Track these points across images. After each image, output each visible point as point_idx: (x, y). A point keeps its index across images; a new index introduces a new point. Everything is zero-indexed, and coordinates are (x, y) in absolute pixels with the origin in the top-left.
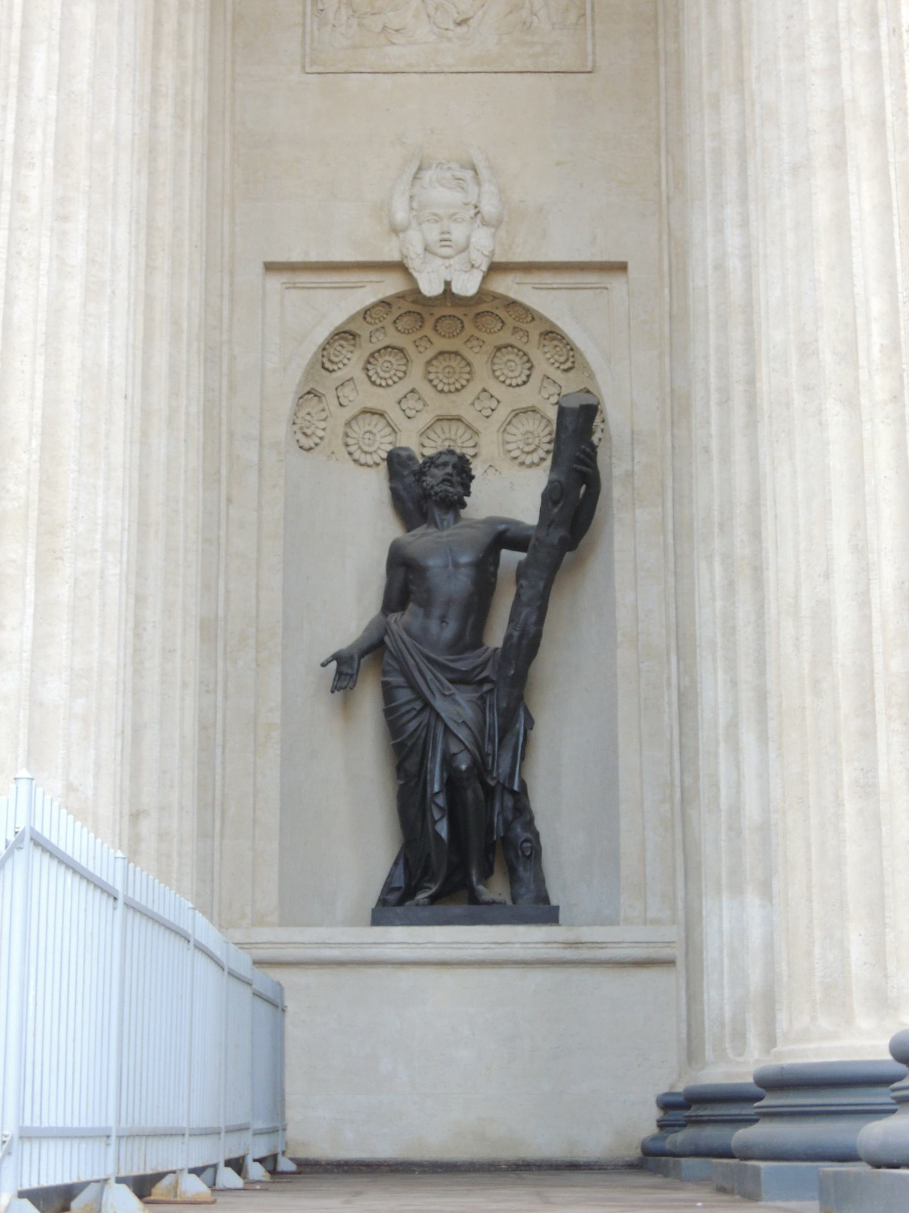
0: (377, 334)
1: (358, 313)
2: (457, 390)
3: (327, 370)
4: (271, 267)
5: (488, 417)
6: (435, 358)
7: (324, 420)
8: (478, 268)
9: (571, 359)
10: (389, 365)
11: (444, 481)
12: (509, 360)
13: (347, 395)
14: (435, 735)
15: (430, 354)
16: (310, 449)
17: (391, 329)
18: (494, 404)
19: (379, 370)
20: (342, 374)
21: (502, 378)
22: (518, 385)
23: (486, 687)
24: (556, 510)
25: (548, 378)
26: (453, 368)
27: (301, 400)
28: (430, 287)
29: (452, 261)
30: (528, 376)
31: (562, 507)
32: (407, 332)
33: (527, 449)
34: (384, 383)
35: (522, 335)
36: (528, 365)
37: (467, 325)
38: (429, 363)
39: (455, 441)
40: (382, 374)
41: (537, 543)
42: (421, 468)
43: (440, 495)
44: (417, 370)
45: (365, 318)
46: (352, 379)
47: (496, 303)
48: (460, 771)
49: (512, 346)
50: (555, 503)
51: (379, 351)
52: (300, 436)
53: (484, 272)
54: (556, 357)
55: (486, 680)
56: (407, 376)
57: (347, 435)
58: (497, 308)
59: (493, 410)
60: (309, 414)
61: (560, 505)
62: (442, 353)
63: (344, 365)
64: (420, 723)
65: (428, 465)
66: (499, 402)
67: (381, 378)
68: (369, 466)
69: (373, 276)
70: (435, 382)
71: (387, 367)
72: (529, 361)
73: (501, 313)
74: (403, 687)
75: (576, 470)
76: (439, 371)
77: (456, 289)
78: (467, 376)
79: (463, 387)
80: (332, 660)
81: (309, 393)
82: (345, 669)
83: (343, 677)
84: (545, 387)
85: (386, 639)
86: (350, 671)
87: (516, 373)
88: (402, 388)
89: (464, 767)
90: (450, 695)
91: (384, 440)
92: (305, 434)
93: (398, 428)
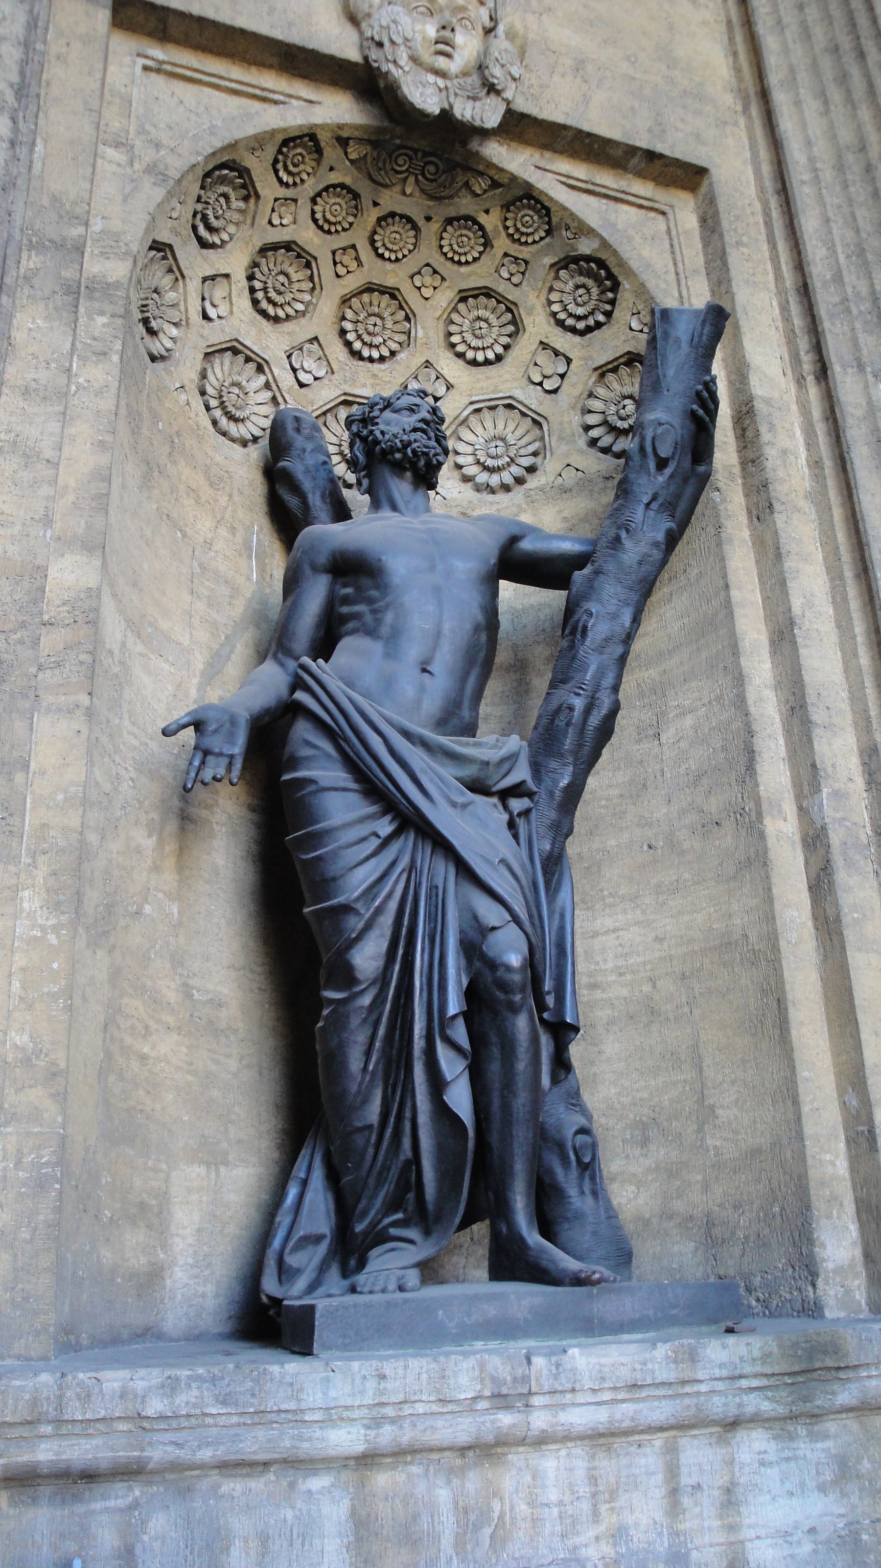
1: (273, 133)
2: (382, 359)
6: (359, 293)
7: (175, 324)
8: (498, 93)
11: (415, 430)
12: (479, 318)
13: (216, 302)
14: (433, 888)
15: (352, 282)
17: (304, 213)
19: (270, 285)
20: (216, 262)
22: (487, 362)
23: (517, 805)
24: (660, 479)
26: (382, 319)
29: (449, 84)
30: (506, 347)
31: (671, 476)
32: (324, 227)
35: (514, 271)
36: (511, 328)
38: (345, 301)
40: (272, 294)
41: (623, 534)
42: (364, 413)
43: (414, 445)
46: (227, 276)
48: (508, 968)
50: (662, 464)
55: (517, 790)
56: (308, 315)
57: (203, 376)
58: (487, 212)
61: (668, 471)
62: (369, 289)
64: (393, 864)
65: (379, 407)
66: (449, 387)
67: (270, 301)
68: (233, 440)
69: (303, 89)
70: (351, 337)
71: (283, 285)
72: (514, 322)
73: (490, 221)
74: (345, 789)
75: (693, 413)
76: (360, 319)
78: (403, 338)
79: (393, 353)
80: (185, 726)
82: (215, 743)
83: (210, 759)
84: (536, 364)
85: (300, 696)
86: (228, 750)
87: (488, 341)
89: (515, 960)
90: (465, 806)
91: (256, 409)
93: (282, 396)
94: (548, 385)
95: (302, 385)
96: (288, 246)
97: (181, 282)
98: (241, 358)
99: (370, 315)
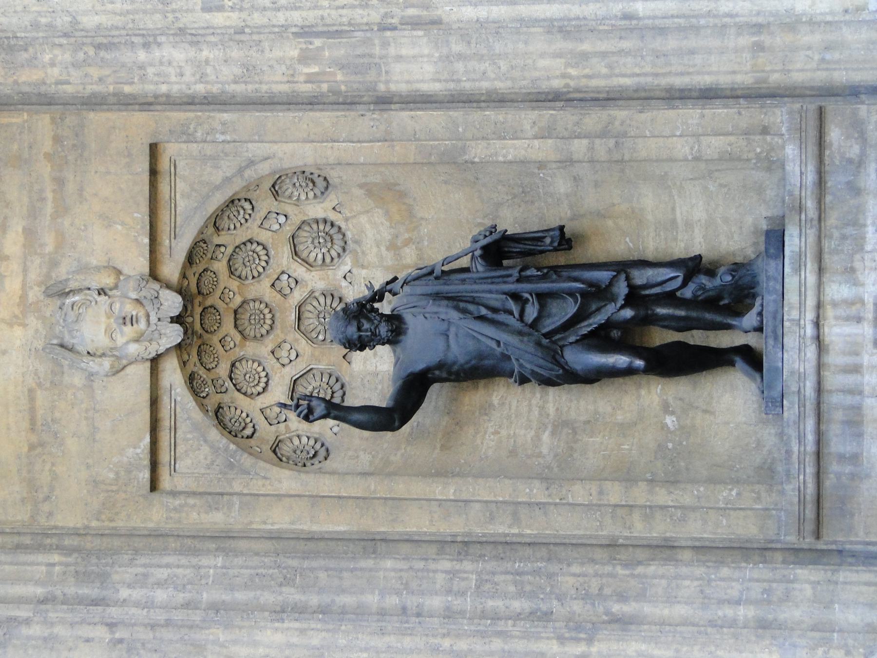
0: (218, 386)
3: (253, 434)
4: (154, 486)
5: (297, 282)
8: (158, 293)
10: (248, 376)
16: (327, 450)
18: (285, 277)
19: (252, 384)
21: (261, 270)
25: (262, 224)
27: (284, 459)
28: (174, 334)
30: (258, 244)
37: (209, 302)
39: (320, 312)
44: (250, 349)
45: (204, 397)
47: (190, 274)
51: (235, 385)
52: (315, 461)
54: (240, 217)
59: (289, 276)
60: (295, 452)
62: (236, 326)
63: (248, 416)
66: (283, 272)
68: (344, 394)
77: (175, 312)
81: (274, 452)
88: (271, 363)
92: (314, 456)
95: (297, 356)
96: (231, 379)
97: (281, 438)
99: (251, 324)
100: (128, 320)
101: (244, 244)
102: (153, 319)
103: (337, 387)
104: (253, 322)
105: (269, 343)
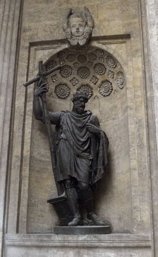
9: (115, 64)
30: (105, 71)
33: (105, 92)
34: (66, 76)
49: (100, 63)
53: (87, 39)
62: (81, 67)
94: (112, 77)
95: (74, 85)
98: (62, 85)
99: (82, 71)
100: (77, 30)
101: (105, 67)
102: (78, 38)
103: (65, 97)
104: (83, 72)
105: (78, 77)
